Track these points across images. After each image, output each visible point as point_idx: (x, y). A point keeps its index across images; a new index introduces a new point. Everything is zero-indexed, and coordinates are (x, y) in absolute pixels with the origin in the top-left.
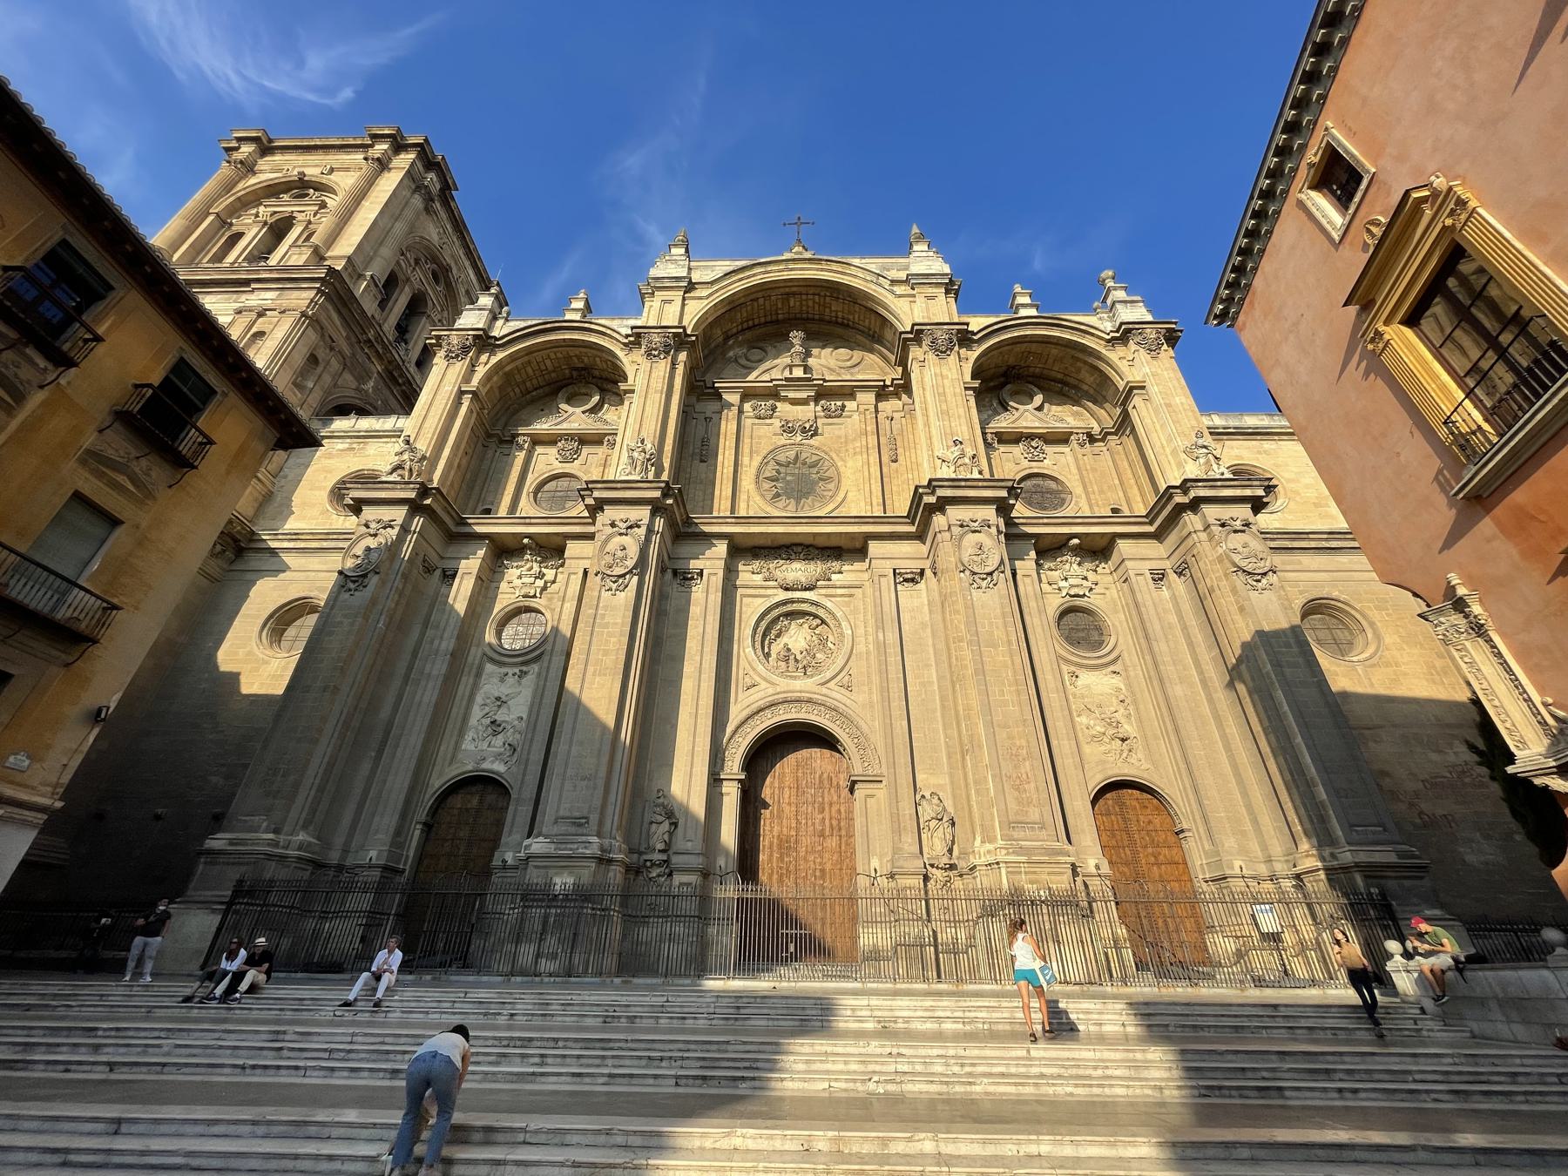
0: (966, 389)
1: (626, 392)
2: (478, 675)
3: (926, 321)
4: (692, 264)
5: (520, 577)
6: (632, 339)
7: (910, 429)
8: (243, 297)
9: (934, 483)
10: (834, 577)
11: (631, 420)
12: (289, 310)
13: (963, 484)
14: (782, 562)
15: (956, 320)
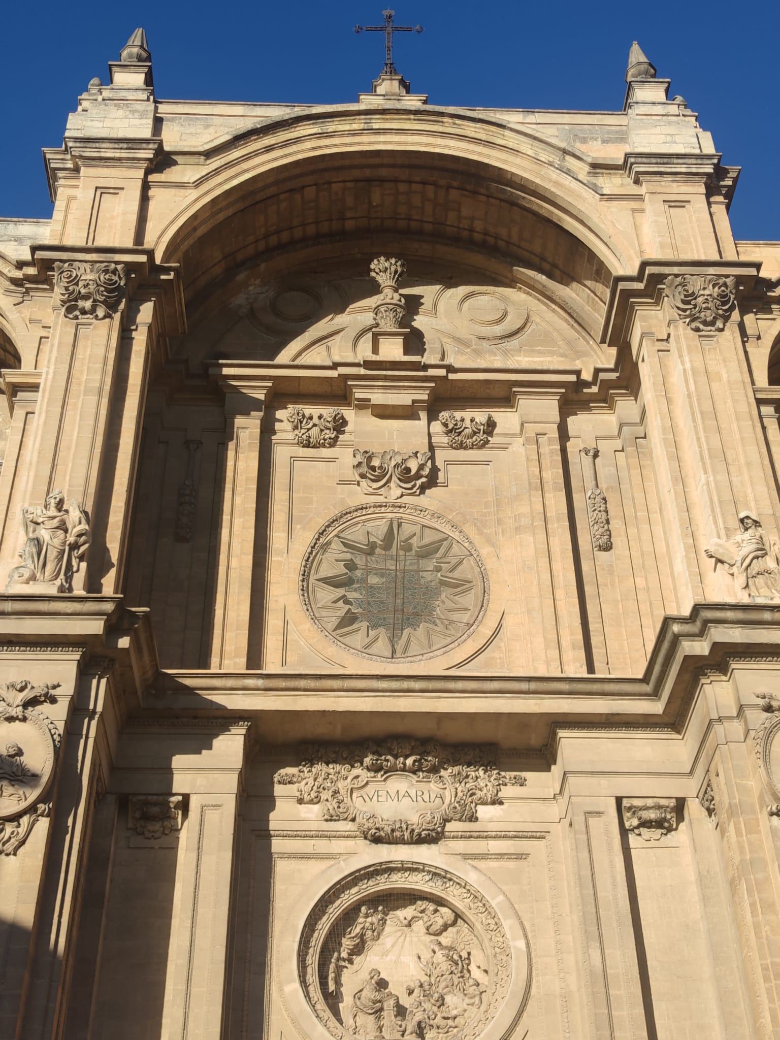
0: (760, 402)
3: (669, 256)
4: (162, 108)
6: (31, 271)
7: (636, 479)
9: (709, 614)
10: (483, 812)
11: (30, 453)
13: (767, 616)
14: (365, 775)
15: (730, 255)
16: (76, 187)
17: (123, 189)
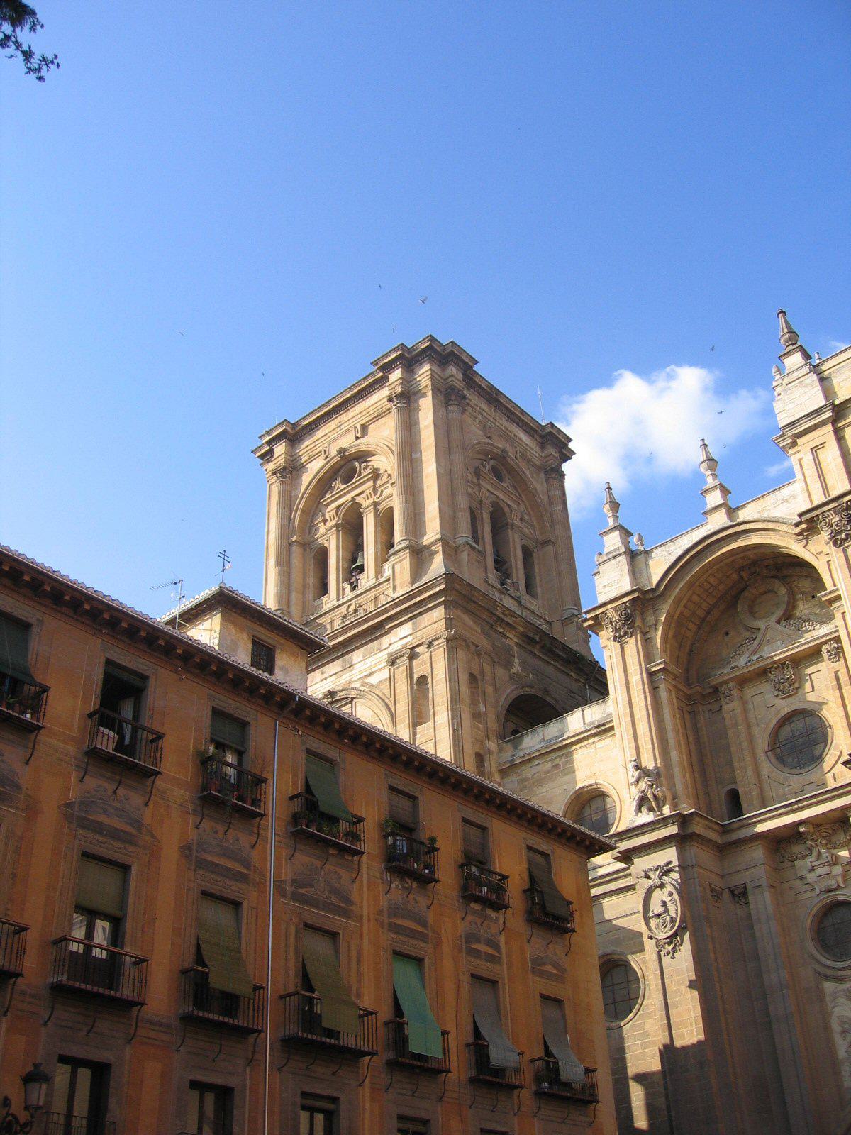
1: (831, 601)
2: (821, 997)
5: (812, 870)
6: (804, 526)
8: (385, 641)
12: (434, 640)
16: (799, 451)
17: (825, 443)
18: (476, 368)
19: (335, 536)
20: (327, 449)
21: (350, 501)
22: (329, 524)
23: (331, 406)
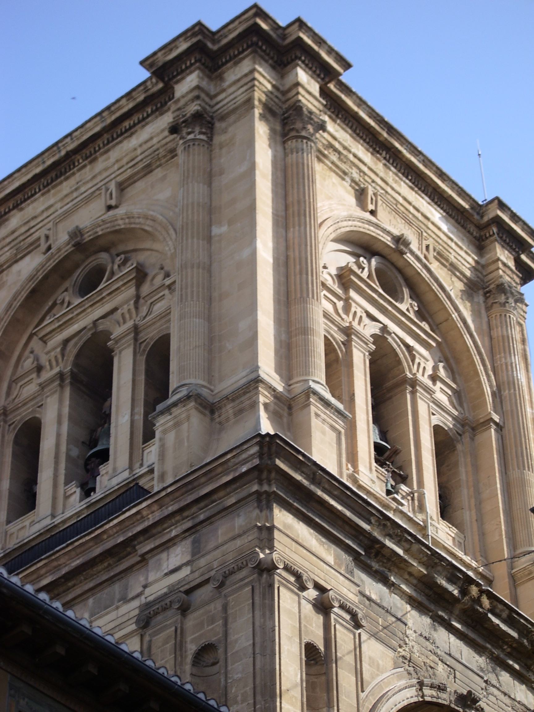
12: (232, 573)
18: (346, 77)
19: (56, 396)
20: (51, 233)
21: (90, 329)
22: (46, 375)
23: (63, 153)
